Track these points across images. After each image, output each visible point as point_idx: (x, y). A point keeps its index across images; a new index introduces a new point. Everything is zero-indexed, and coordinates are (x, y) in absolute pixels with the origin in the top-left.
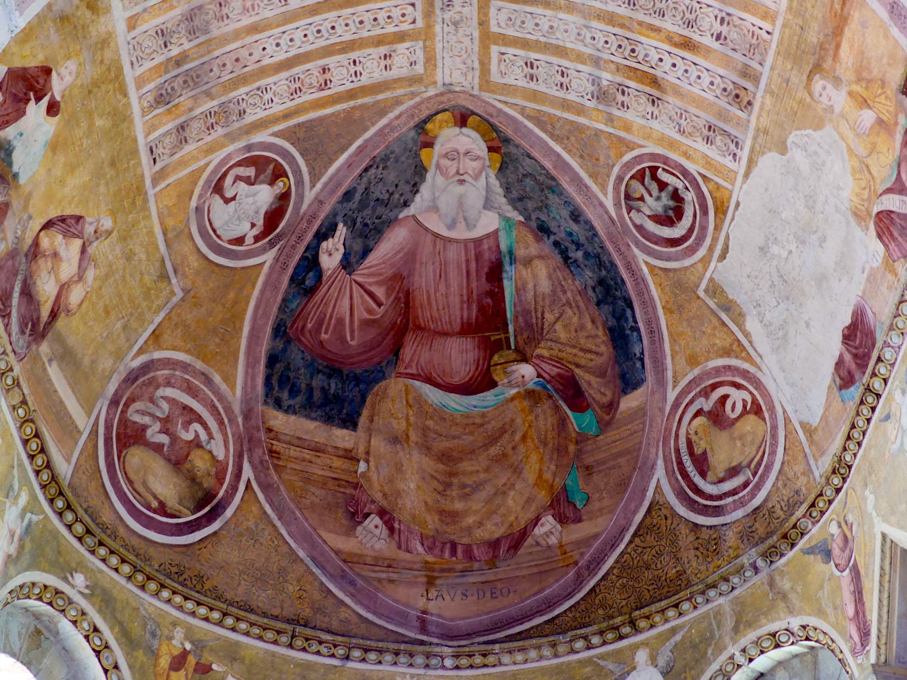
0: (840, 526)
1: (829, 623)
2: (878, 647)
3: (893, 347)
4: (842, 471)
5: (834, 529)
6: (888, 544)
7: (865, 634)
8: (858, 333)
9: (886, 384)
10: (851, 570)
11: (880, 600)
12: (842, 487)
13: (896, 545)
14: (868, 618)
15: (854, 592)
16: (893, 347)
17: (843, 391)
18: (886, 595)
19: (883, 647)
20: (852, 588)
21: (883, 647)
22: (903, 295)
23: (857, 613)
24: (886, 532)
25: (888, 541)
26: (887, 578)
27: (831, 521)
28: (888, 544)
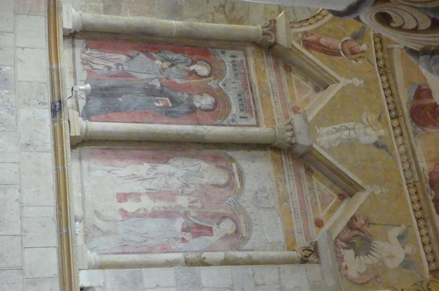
0: (362, 52)
1: (326, 23)
2: (298, 50)
3: (401, 145)
4: (382, 70)
5: (364, 47)
6: (334, 81)
7: (308, 45)
8: (430, 116)
9: (392, 126)
10: (339, 50)
11: (315, 63)
12: (377, 62)
13: (331, 84)
14: (313, 52)
15: (328, 48)
16: (401, 145)
17: (417, 87)
18: (316, 67)
19: (297, 52)
20: (331, 47)
21: (297, 52)
22: (411, 170)
23: (320, 45)
24: (340, 83)
25: (335, 82)
26: (322, 72)
27: (368, 47)
28: (334, 81)
